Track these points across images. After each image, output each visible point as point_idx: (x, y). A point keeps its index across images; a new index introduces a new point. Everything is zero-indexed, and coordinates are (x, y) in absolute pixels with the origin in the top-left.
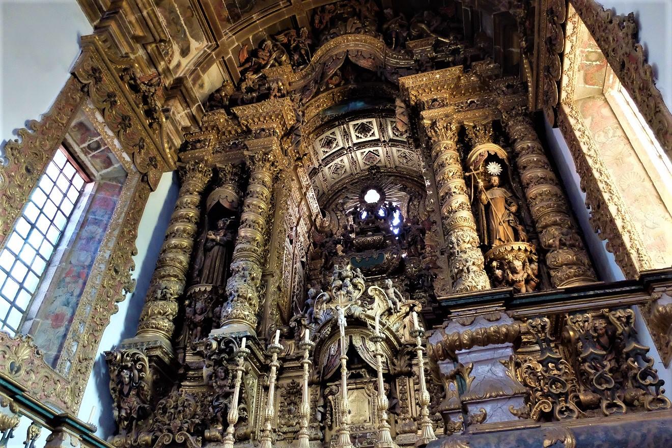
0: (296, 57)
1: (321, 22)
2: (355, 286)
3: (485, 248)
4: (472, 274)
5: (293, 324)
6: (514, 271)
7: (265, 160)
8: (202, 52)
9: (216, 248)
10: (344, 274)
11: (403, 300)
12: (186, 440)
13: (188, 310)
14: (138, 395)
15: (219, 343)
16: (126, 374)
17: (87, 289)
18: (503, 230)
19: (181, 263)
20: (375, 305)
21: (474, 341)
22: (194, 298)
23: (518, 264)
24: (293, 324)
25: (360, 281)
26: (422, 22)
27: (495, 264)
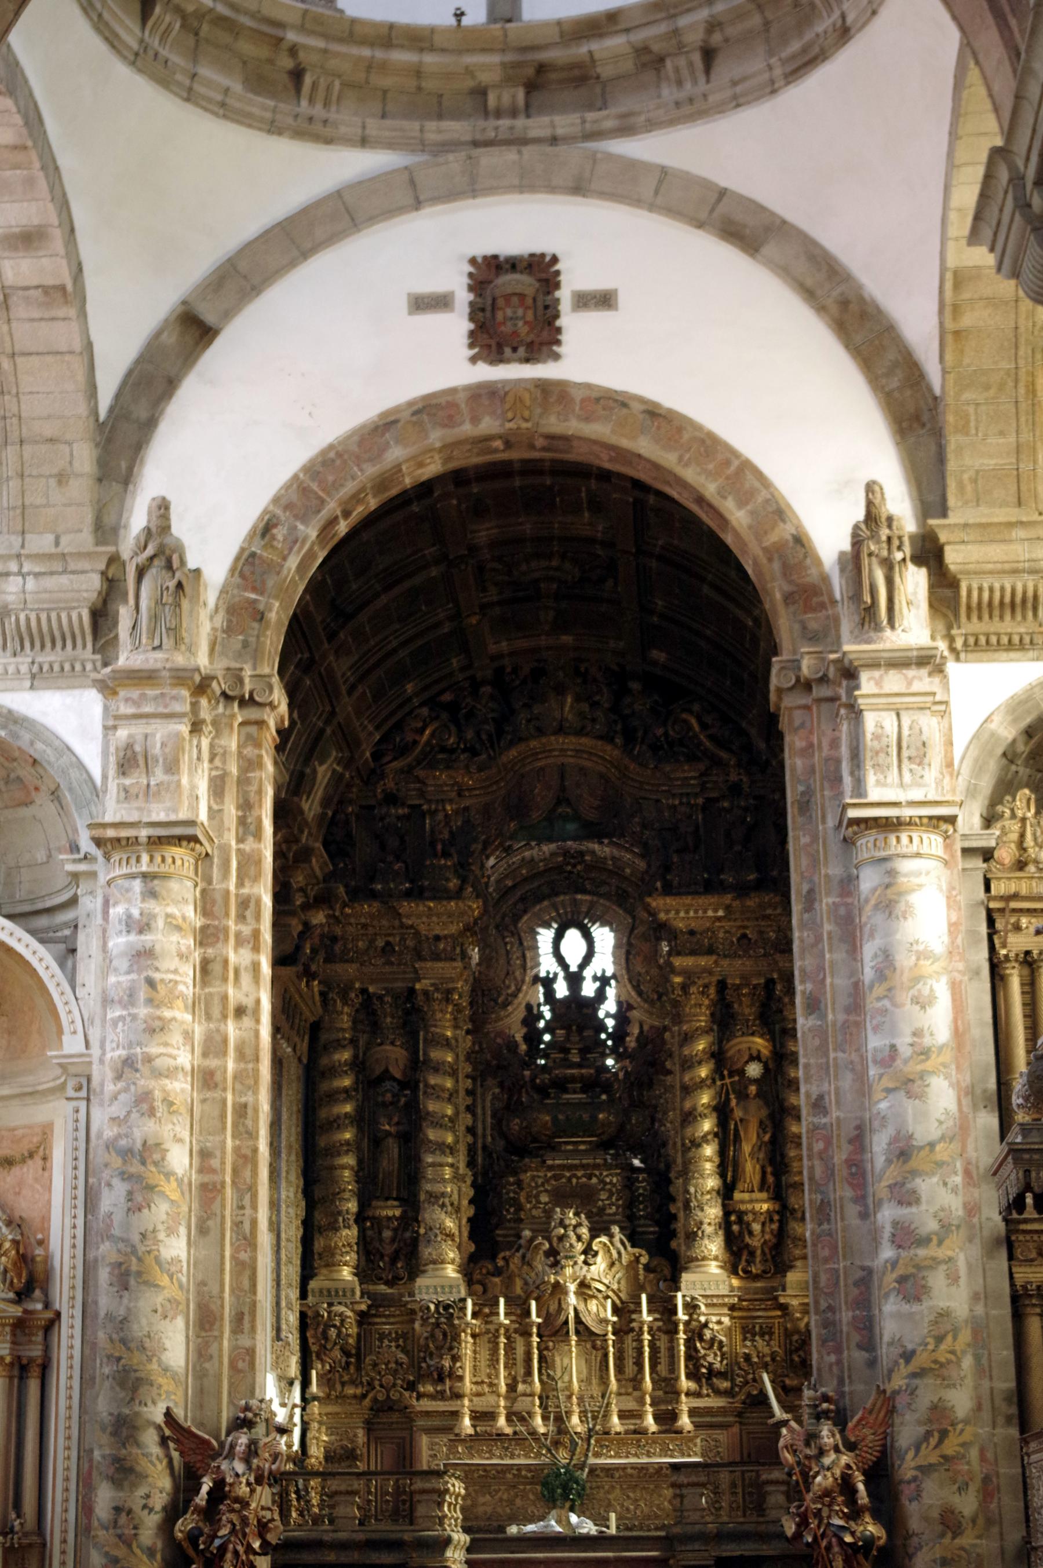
0: (470, 734)
1: (515, 670)
2: (579, 1238)
3: (726, 1192)
4: (706, 1241)
5: (501, 1263)
6: (751, 1233)
7: (448, 1000)
8: (329, 774)
9: (390, 1140)
10: (567, 1222)
11: (629, 1248)
12: (401, 1394)
13: (369, 1233)
14: (342, 1349)
15: (437, 1306)
16: (333, 1333)
17: (283, 1244)
18: (751, 1169)
19: (352, 1168)
20: (599, 1258)
21: (689, 1485)
22: (379, 1223)
23: (756, 1227)
24: (501, 1263)
25: (584, 1231)
26: (690, 711)
27: (733, 1218)
